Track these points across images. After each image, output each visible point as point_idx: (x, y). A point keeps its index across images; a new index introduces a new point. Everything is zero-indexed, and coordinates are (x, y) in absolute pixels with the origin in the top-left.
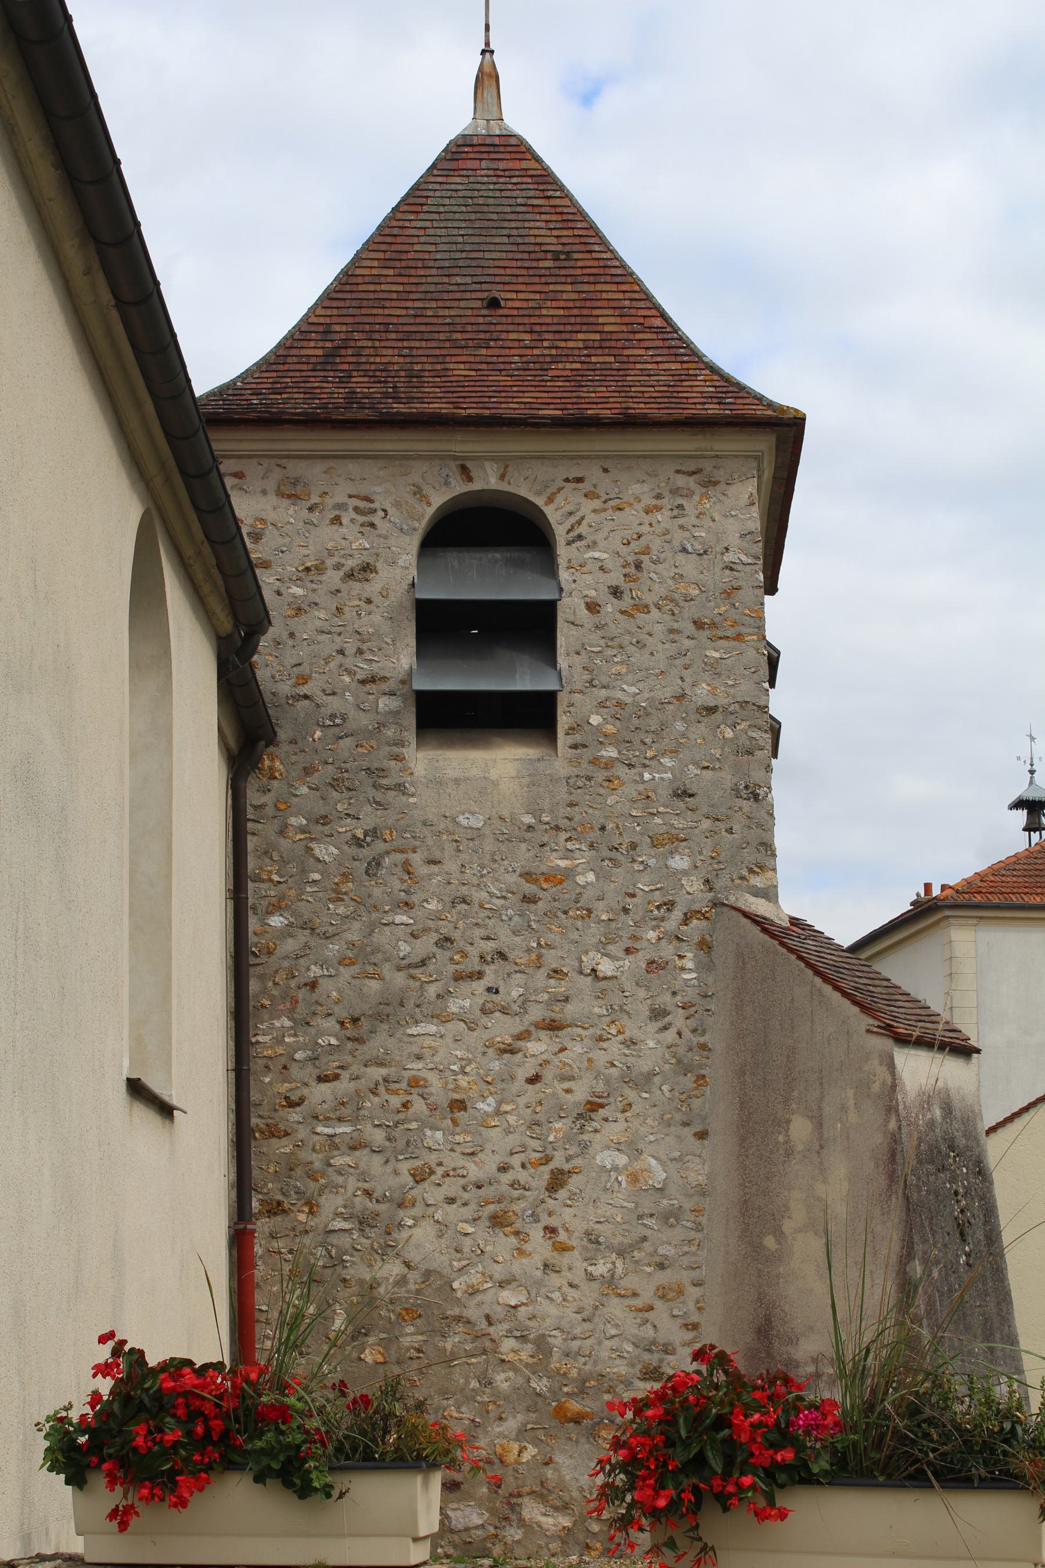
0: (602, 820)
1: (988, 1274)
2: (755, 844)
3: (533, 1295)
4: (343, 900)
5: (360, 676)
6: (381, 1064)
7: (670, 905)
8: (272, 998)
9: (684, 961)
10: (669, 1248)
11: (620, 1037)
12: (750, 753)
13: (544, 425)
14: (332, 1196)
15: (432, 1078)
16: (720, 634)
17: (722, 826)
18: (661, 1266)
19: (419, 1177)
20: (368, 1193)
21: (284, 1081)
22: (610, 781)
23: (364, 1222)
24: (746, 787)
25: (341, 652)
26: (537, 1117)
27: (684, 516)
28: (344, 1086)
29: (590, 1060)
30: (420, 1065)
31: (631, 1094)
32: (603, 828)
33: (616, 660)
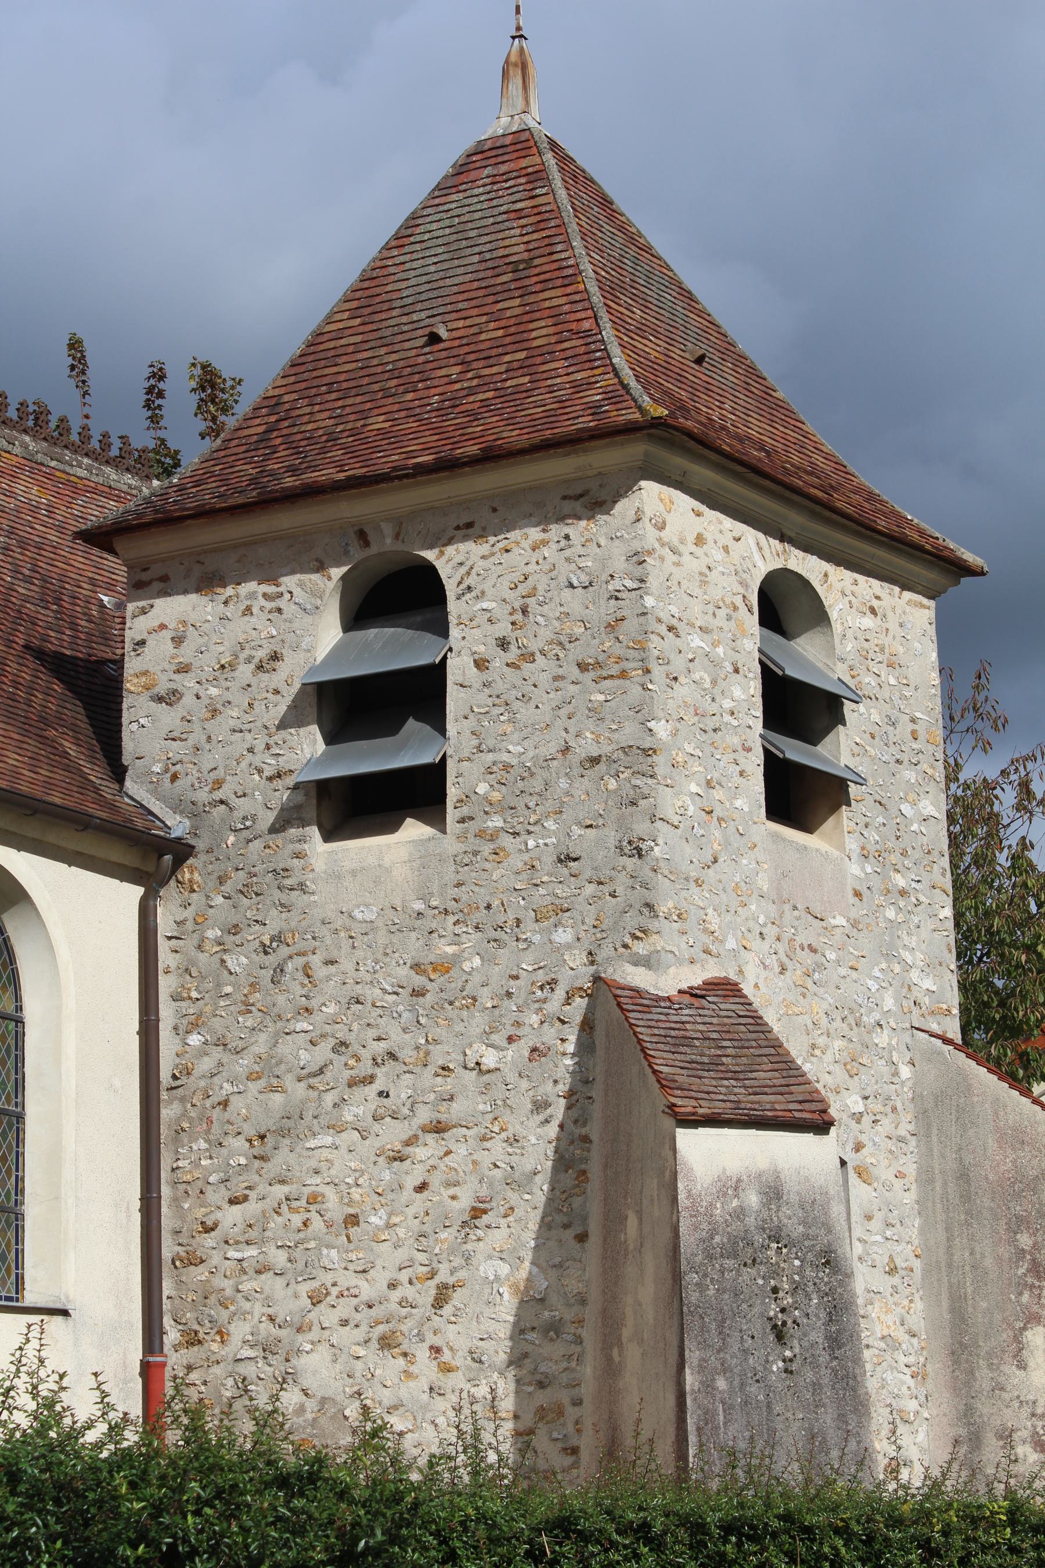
1: (825, 1381)
2: (637, 906)
3: (419, 1421)
4: (250, 1012)
5: (268, 772)
6: (282, 1182)
7: (552, 983)
8: (191, 1120)
9: (566, 1045)
10: (550, 1364)
11: (504, 1135)
12: (633, 804)
13: (407, 476)
14: (241, 1323)
15: (330, 1192)
16: (605, 673)
17: (606, 889)
18: (541, 1385)
19: (316, 1300)
20: (272, 1319)
21: (201, 1206)
23: (268, 1349)
24: (630, 842)
25: (251, 750)
26: (424, 1228)
27: (570, 546)
28: (252, 1208)
29: (475, 1163)
31: (513, 1197)
32: (488, 907)
33: (502, 718)
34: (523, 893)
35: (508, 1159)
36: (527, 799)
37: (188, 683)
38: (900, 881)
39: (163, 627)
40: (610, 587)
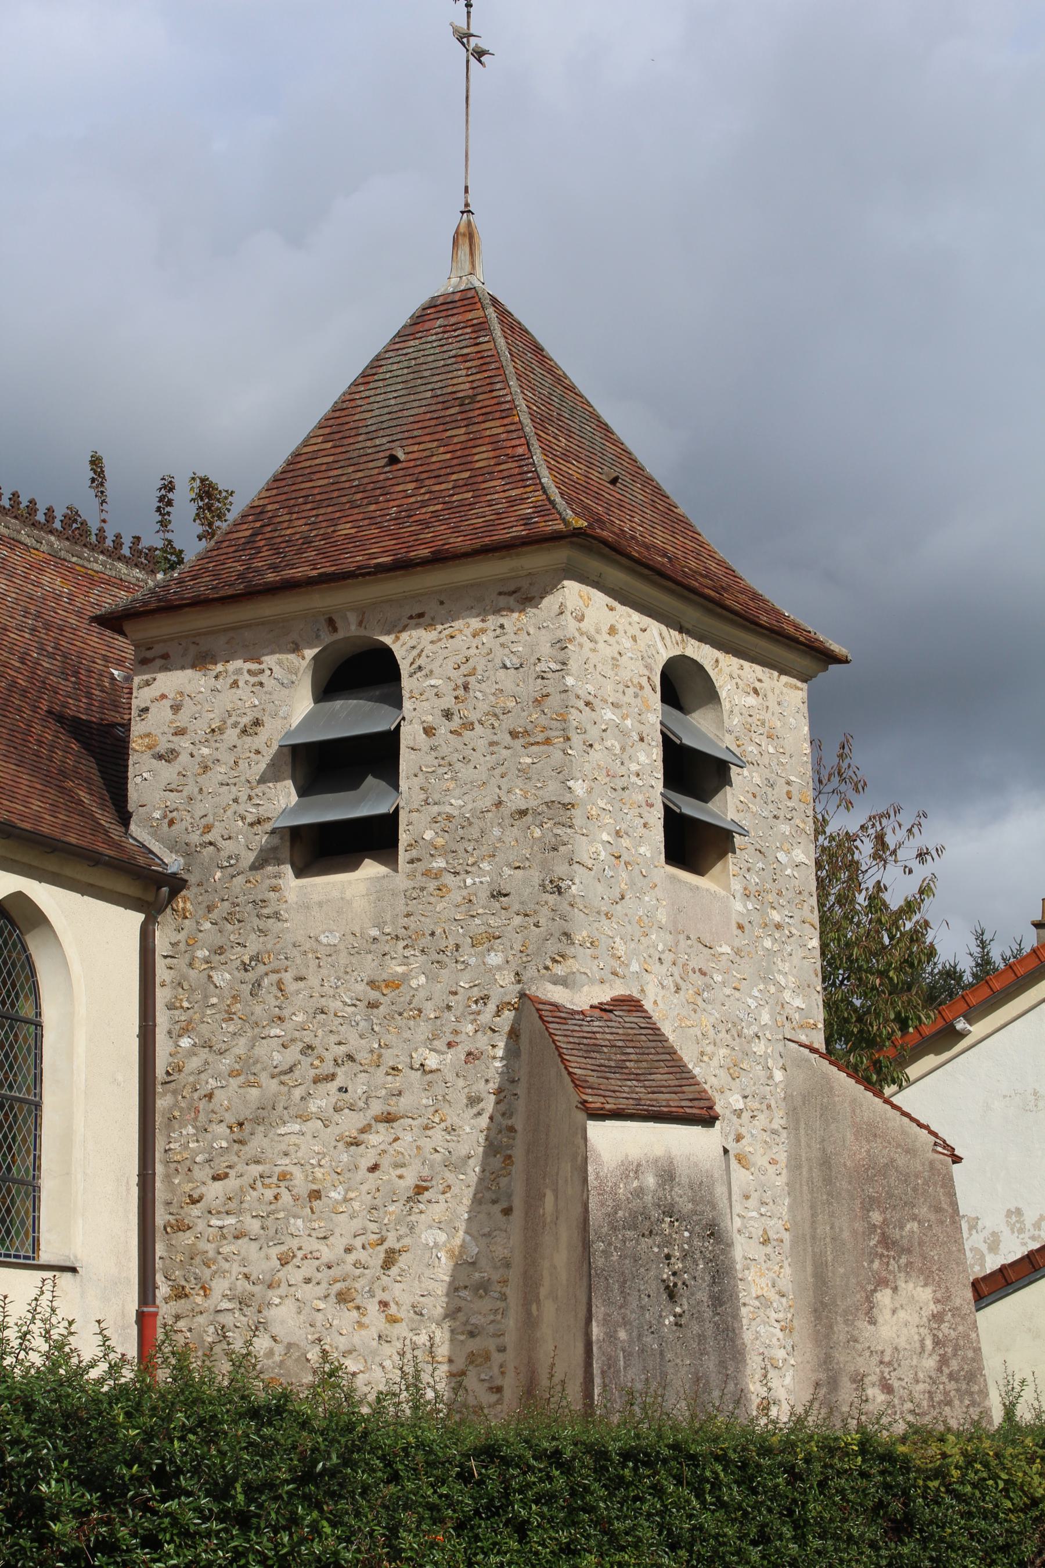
0: (432, 927)
1: (709, 1333)
2: (557, 935)
3: (369, 1363)
4: (232, 1019)
5: (249, 820)
6: (258, 1162)
7: (485, 999)
8: (181, 1110)
9: (496, 1050)
10: (479, 1317)
11: (443, 1125)
12: (555, 849)
13: (369, 574)
14: (221, 1280)
15: (297, 1172)
16: (532, 740)
17: (531, 920)
18: (472, 1334)
19: (284, 1261)
20: (247, 1277)
22: (439, 889)
23: (243, 1302)
24: (551, 882)
25: (236, 801)
26: (376, 1202)
27: (504, 634)
28: (232, 1183)
29: (418, 1148)
30: (287, 1161)
31: (450, 1177)
32: (433, 934)
33: (446, 776)
34: (461, 923)
35: (446, 1145)
36: (466, 844)
37: (183, 744)
38: (776, 916)
39: (163, 696)
40: (538, 669)
